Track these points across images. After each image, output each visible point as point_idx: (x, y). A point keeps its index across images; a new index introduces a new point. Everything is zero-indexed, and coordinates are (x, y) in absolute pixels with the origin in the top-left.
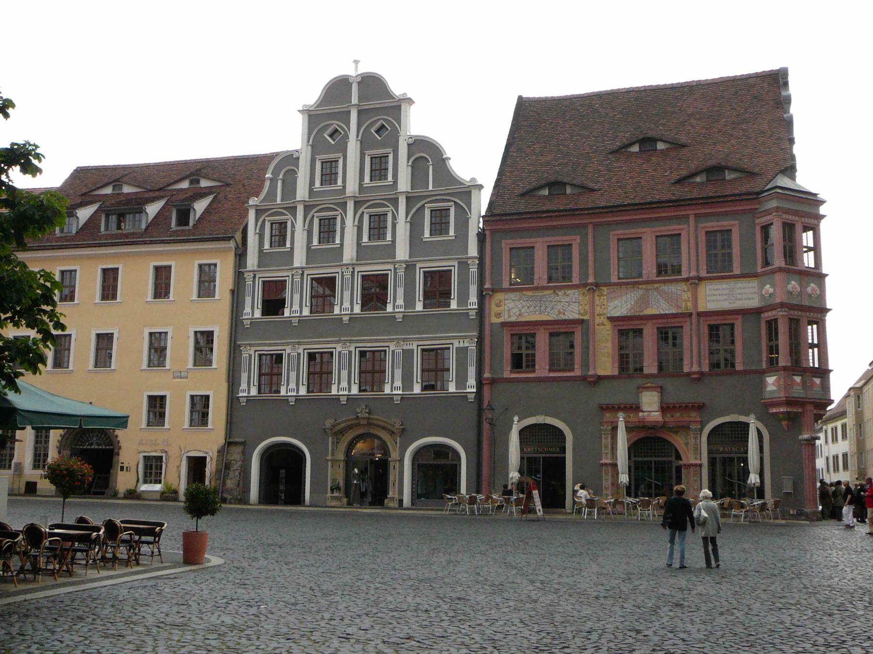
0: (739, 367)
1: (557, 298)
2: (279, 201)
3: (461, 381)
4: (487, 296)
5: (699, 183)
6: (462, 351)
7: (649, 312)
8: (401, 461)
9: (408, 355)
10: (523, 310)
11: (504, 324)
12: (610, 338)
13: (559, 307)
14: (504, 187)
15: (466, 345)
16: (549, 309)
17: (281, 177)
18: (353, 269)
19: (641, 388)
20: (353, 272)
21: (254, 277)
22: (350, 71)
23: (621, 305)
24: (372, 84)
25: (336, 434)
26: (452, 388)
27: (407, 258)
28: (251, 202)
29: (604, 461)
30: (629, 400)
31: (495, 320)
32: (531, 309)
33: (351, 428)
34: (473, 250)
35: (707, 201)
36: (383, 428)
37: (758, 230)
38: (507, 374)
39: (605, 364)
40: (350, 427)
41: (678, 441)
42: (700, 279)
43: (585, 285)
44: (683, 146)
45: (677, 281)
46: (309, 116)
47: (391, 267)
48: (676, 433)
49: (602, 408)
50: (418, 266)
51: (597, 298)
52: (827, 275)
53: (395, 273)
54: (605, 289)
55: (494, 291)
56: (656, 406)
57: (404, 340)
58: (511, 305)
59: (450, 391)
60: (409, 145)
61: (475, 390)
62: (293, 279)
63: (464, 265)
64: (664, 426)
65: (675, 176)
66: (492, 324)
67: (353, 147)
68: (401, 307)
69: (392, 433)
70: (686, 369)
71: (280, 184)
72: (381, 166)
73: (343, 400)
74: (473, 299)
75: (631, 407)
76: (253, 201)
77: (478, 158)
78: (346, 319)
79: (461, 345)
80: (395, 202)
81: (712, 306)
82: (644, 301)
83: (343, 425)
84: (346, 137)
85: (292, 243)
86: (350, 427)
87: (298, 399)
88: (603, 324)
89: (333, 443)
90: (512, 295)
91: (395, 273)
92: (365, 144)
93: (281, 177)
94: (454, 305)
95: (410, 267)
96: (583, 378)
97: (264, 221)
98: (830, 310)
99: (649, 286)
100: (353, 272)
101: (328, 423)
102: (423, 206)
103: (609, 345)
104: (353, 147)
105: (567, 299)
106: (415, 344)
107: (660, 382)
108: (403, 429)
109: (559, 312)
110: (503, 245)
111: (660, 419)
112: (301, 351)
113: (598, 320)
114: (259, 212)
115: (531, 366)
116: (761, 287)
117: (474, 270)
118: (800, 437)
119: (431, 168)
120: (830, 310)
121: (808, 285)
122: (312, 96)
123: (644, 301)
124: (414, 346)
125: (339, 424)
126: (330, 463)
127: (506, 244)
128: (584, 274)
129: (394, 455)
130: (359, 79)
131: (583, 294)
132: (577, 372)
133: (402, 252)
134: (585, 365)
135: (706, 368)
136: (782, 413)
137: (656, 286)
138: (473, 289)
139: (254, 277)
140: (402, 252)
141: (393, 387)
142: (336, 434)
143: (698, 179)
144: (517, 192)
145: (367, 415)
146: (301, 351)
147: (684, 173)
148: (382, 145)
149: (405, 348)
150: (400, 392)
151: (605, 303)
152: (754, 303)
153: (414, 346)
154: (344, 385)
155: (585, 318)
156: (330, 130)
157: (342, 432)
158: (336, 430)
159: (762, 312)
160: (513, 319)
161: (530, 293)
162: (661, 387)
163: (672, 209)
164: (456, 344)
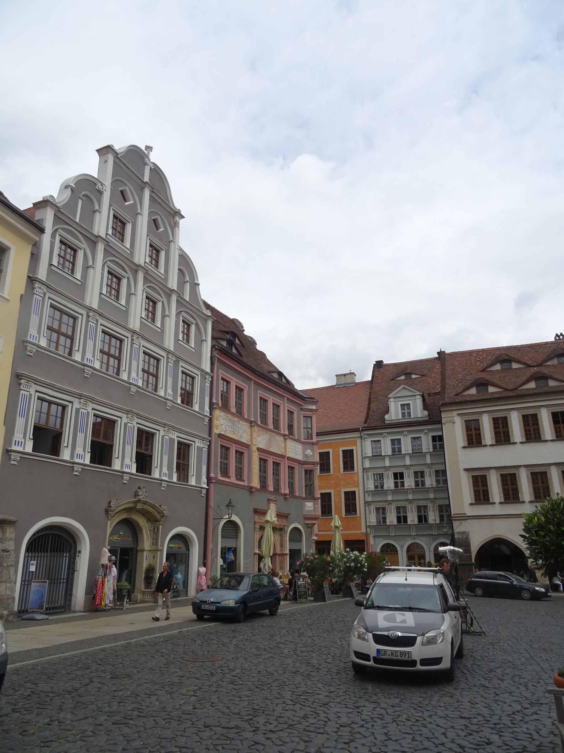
6: (200, 449)
7: (271, 450)
11: (220, 435)
16: (236, 432)
37: (302, 416)
44: (243, 346)
74: (207, 408)
90: (222, 414)
116: (304, 450)
117: (208, 385)
137: (274, 434)
152: (300, 457)
160: (223, 433)
161: (230, 416)
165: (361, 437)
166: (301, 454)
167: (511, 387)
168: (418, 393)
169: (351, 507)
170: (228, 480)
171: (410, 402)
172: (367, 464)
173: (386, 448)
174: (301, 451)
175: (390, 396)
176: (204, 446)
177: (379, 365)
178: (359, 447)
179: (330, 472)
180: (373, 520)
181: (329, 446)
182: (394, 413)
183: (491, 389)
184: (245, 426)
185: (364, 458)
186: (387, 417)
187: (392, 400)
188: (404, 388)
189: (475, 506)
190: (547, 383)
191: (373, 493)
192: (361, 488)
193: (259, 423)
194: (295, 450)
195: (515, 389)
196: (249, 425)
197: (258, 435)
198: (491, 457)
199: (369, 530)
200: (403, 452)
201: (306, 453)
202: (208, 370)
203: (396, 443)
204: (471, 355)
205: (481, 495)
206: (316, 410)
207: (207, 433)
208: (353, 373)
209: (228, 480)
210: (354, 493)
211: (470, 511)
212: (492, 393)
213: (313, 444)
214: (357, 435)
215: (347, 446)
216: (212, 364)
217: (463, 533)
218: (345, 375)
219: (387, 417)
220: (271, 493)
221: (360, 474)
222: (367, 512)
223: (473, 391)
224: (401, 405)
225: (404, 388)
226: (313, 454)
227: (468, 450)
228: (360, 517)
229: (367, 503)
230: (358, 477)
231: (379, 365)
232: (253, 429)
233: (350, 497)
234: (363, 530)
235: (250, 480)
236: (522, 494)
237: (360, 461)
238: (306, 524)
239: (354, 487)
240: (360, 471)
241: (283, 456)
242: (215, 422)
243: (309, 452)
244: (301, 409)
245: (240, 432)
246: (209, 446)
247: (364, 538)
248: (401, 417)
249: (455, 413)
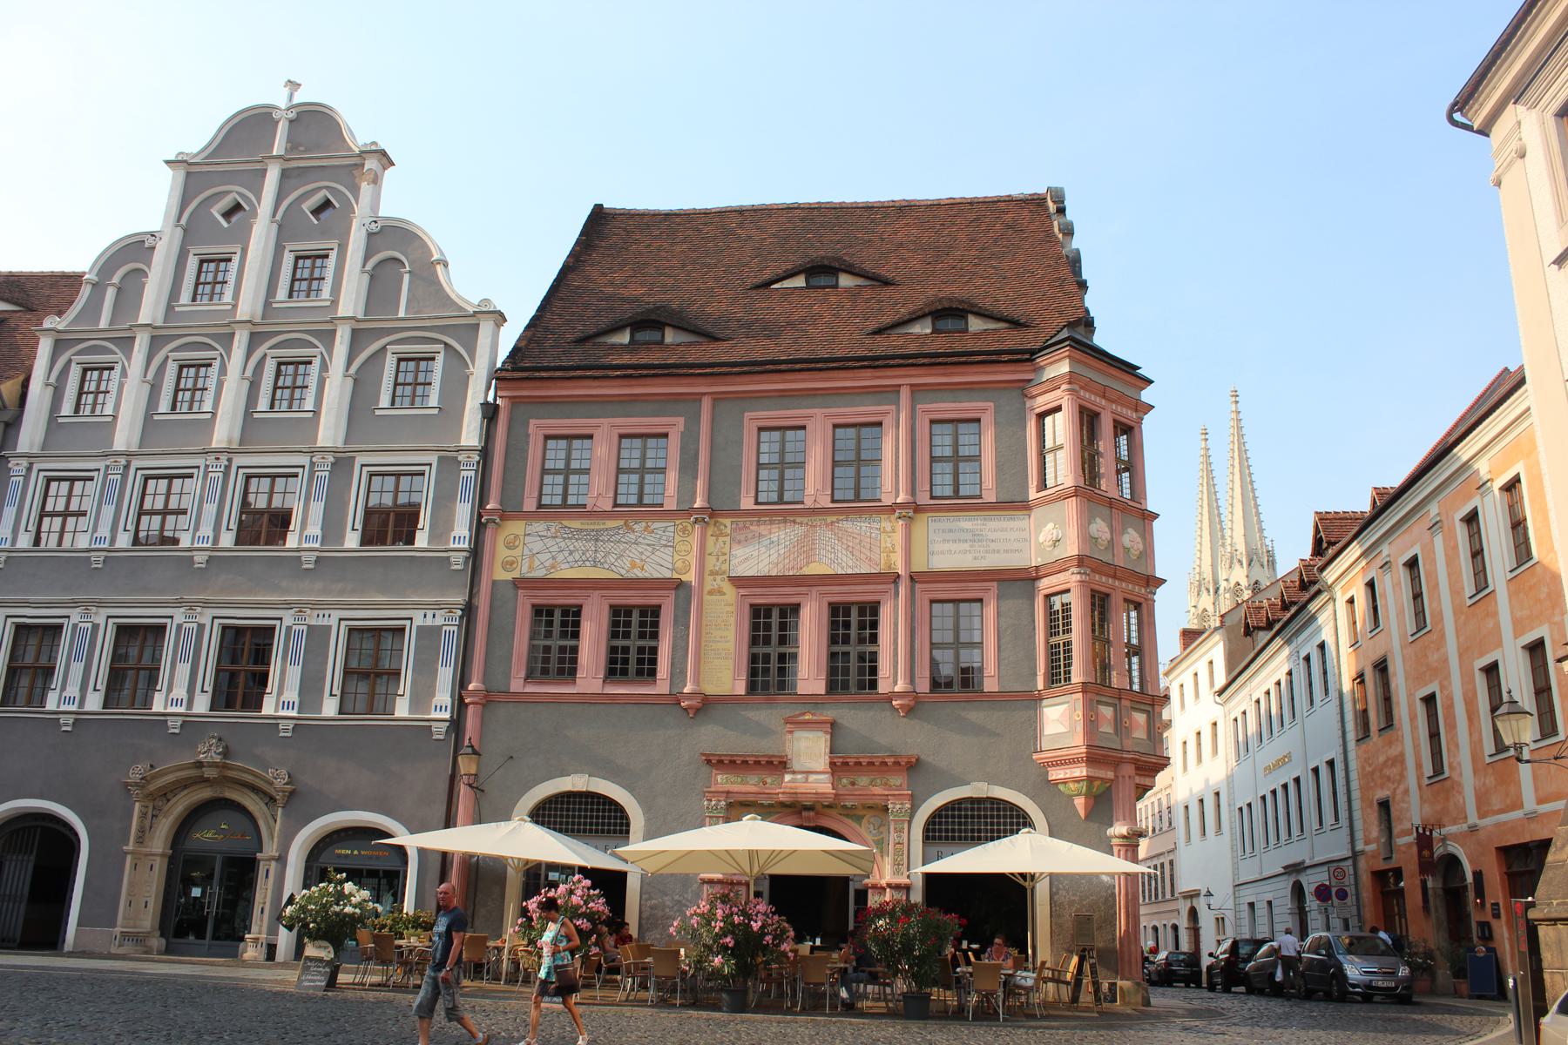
0: (990, 685)
2: (103, 324)
3: (422, 697)
4: (490, 525)
5: (919, 336)
6: (429, 635)
8: (282, 860)
9: (318, 636)
10: (560, 557)
11: (519, 584)
12: (732, 620)
13: (634, 552)
14: (547, 329)
15: (439, 621)
17: (116, 280)
18: (230, 460)
19: (796, 723)
20: (228, 467)
21: (29, 469)
22: (278, 98)
23: (764, 553)
24: (315, 122)
25: (151, 796)
26: (402, 709)
27: (340, 444)
28: (47, 324)
31: (502, 575)
33: (186, 787)
34: (470, 434)
35: (935, 360)
36: (255, 789)
38: (517, 685)
39: (723, 672)
40: (185, 784)
42: (918, 509)
43: (689, 511)
44: (886, 283)
46: (188, 174)
47: (304, 460)
48: (859, 819)
49: (709, 762)
50: (360, 459)
51: (710, 540)
52: (1156, 516)
53: (312, 473)
54: (727, 522)
55: (504, 515)
56: (822, 763)
57: (315, 606)
59: (398, 714)
60: (370, 235)
61: (447, 716)
62: (106, 475)
63: (449, 463)
65: (873, 325)
66: (494, 582)
67: (261, 233)
68: (315, 538)
69: (271, 800)
70: (883, 687)
71: (110, 294)
72: (312, 273)
73: (174, 726)
74: (461, 529)
75: (770, 763)
76: (50, 322)
77: (504, 272)
78: (200, 558)
79: (429, 622)
80: (328, 337)
81: (942, 563)
82: (806, 548)
83: (170, 778)
84: (254, 214)
85: (117, 407)
86: (185, 784)
87: (82, 721)
88: (720, 592)
89: (143, 815)
90: (539, 527)
91: (312, 473)
92: (285, 230)
93: (116, 280)
94: (421, 540)
95: (342, 464)
96: (674, 699)
97: (70, 361)
98: (1164, 581)
99: (817, 520)
100: (228, 467)
101: (135, 774)
102: (384, 348)
103: (731, 634)
104: (261, 233)
105: (650, 539)
106: (336, 615)
107: (829, 714)
108: (292, 793)
109: (633, 565)
110: (531, 429)
112: (101, 620)
113: (710, 583)
114: (60, 345)
115: (567, 668)
117: (469, 473)
118: (1110, 831)
119: (406, 278)
120: (1164, 581)
121: (1123, 531)
122: (196, 138)
124: (332, 619)
125: (154, 777)
126: (129, 858)
127: (536, 427)
128: (686, 491)
129: (270, 849)
130: (291, 115)
131: (684, 530)
132: (662, 686)
133: (330, 432)
134: (678, 673)
135: (924, 686)
136: (1077, 781)
137: (830, 519)
138: (463, 513)
139: (29, 469)
140: (330, 432)
141: (281, 699)
142: (151, 796)
144: (570, 337)
145: (218, 759)
146: (101, 620)
147: (887, 320)
148: (325, 233)
149: (314, 622)
150: (294, 714)
151: (727, 550)
153: (332, 619)
154: (182, 692)
155: (684, 578)
156: (225, 203)
157: (166, 794)
158: (152, 787)
159: (1038, 578)
164: (419, 620)
176: (448, 622)
238: (1056, 783)
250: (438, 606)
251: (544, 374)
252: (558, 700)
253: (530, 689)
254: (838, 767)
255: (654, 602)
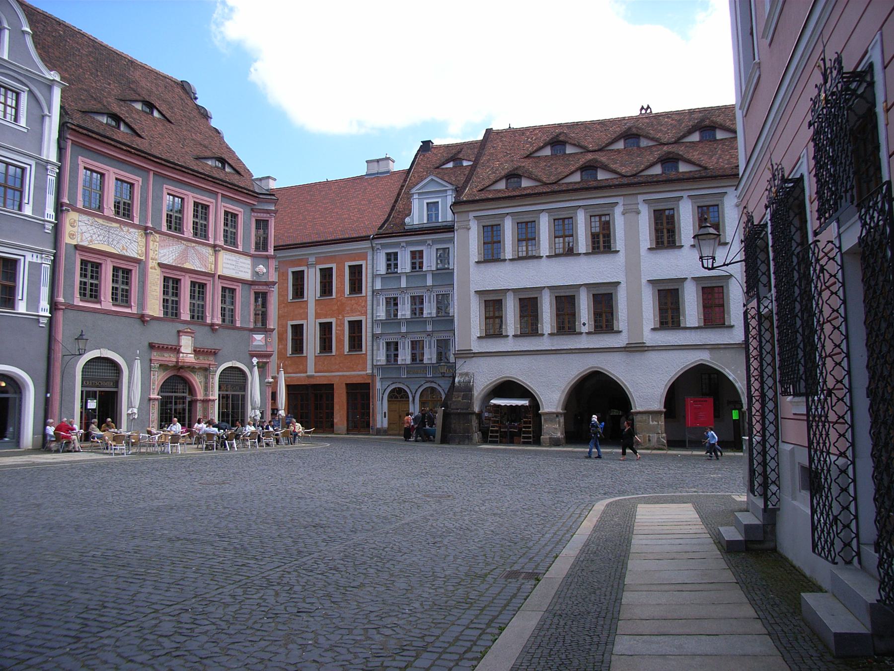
0: (238, 324)
1: (122, 233)
3: (33, 301)
7: (187, 266)
10: (94, 238)
11: (76, 247)
16: (115, 242)
29: (152, 396)
30: (170, 341)
32: (101, 238)
37: (253, 220)
38: (78, 302)
39: (154, 308)
41: (197, 380)
45: (203, 244)
48: (194, 372)
54: (157, 236)
58: (84, 229)
59: (20, 311)
64: (192, 369)
74: (50, 210)
79: (35, 260)
90: (85, 218)
99: (189, 244)
111: (193, 360)
116: (254, 266)
117: (52, 178)
123: (184, 255)
128: (144, 217)
132: (134, 310)
137: (193, 244)
138: (50, 200)
143: (210, 163)
152: (248, 276)
160: (85, 244)
161: (100, 221)
162: (179, 332)
163: (211, 184)
165: (373, 248)
166: (250, 271)
167: (553, 179)
168: (450, 187)
169: (356, 342)
170: (98, 306)
171: (439, 200)
172: (378, 286)
173: (405, 264)
174: (250, 267)
175: (414, 191)
177: (426, 146)
178: (370, 262)
179: (332, 295)
180: (381, 358)
181: (331, 259)
182: (418, 216)
183: (525, 183)
184: (136, 234)
185: (374, 276)
186: (407, 220)
187: (416, 196)
188: (432, 180)
189: (484, 340)
190: (596, 174)
191: (383, 323)
192: (369, 316)
193: (164, 229)
194: (236, 266)
195: (555, 183)
196: (142, 232)
197: (161, 247)
198: (508, 277)
199: (375, 371)
200: (424, 269)
201: (257, 269)
202: (53, 158)
203: (416, 257)
204: (523, 134)
205: (493, 326)
206: (275, 212)
207: (52, 245)
208: (388, 159)
209: (98, 306)
210: (360, 322)
211: (476, 347)
212: (525, 188)
213: (268, 257)
214: (366, 244)
215: (355, 260)
216: (61, 150)
217: (467, 374)
218: (378, 161)
219: (407, 220)
220: (185, 322)
221: (369, 298)
222: (375, 348)
223: (502, 185)
224: (428, 204)
225: (432, 180)
226: (268, 272)
227: (482, 266)
228: (366, 354)
229: (375, 337)
230: (366, 301)
231: (426, 146)
232: (151, 238)
233: (356, 327)
234: (369, 371)
235: (142, 304)
236: (542, 324)
237: (370, 280)
239: (362, 314)
240: (370, 293)
241: (212, 275)
242: (67, 229)
243: (261, 268)
244: (252, 210)
245: (127, 242)
246: (54, 262)
247: (370, 381)
248: (425, 221)
249: (472, 215)
250: (42, 252)
251: (94, 135)
252: (95, 311)
253: (81, 304)
254: (197, 352)
255: (130, 268)
